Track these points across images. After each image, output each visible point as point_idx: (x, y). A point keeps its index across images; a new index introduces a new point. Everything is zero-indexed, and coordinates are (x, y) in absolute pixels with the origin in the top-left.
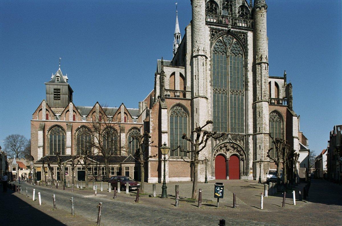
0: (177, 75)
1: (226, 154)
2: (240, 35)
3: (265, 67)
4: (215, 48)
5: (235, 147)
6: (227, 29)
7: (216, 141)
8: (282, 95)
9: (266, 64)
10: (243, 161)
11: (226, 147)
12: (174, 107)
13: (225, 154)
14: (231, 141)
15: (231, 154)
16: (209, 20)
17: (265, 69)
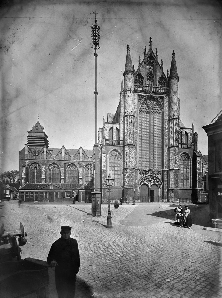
0: (114, 129)
1: (148, 184)
2: (159, 99)
3: (176, 122)
4: (141, 109)
5: (155, 179)
6: (149, 95)
7: (141, 174)
8: (190, 140)
9: (178, 120)
10: (161, 188)
11: (148, 179)
12: (111, 152)
13: (147, 184)
14: (152, 175)
15: (152, 184)
16: (136, 89)
17: (176, 123)
